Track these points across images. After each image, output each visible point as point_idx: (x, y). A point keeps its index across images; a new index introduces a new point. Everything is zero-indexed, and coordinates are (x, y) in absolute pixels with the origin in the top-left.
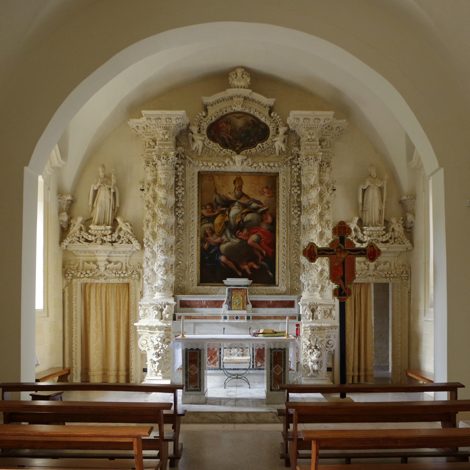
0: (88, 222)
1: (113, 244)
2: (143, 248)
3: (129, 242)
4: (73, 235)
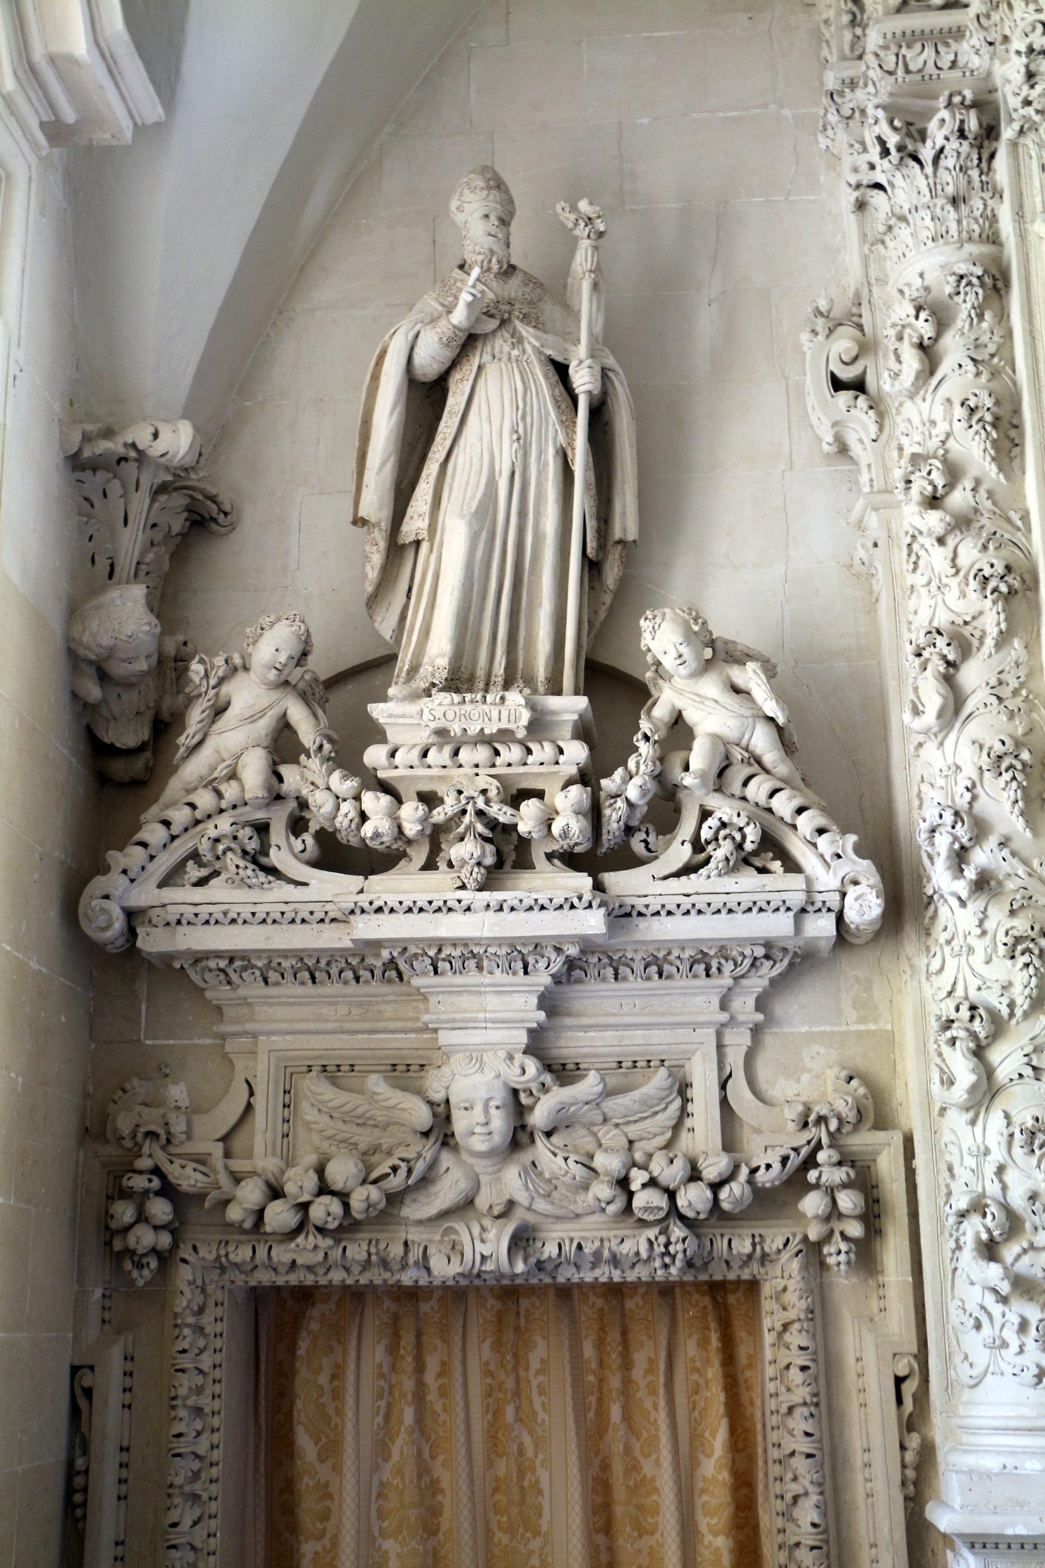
0: (345, 688)
1: (610, 878)
2: (905, 906)
3: (770, 849)
4: (205, 800)
